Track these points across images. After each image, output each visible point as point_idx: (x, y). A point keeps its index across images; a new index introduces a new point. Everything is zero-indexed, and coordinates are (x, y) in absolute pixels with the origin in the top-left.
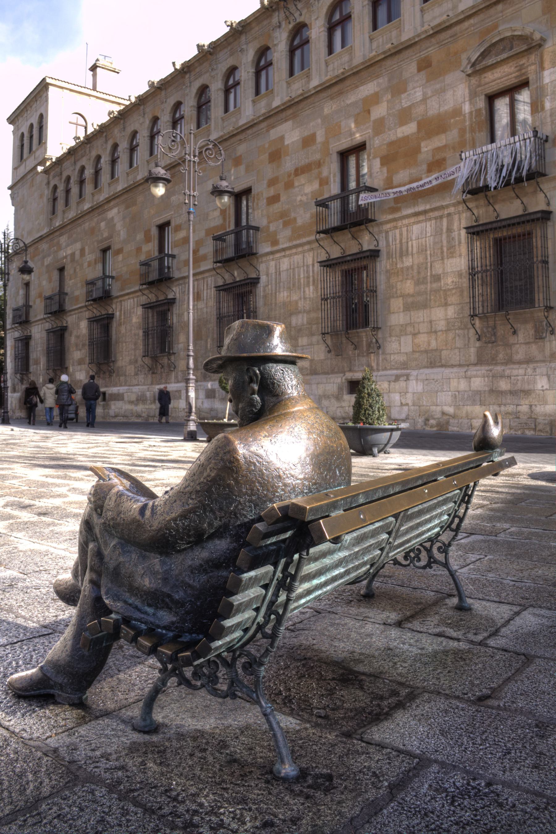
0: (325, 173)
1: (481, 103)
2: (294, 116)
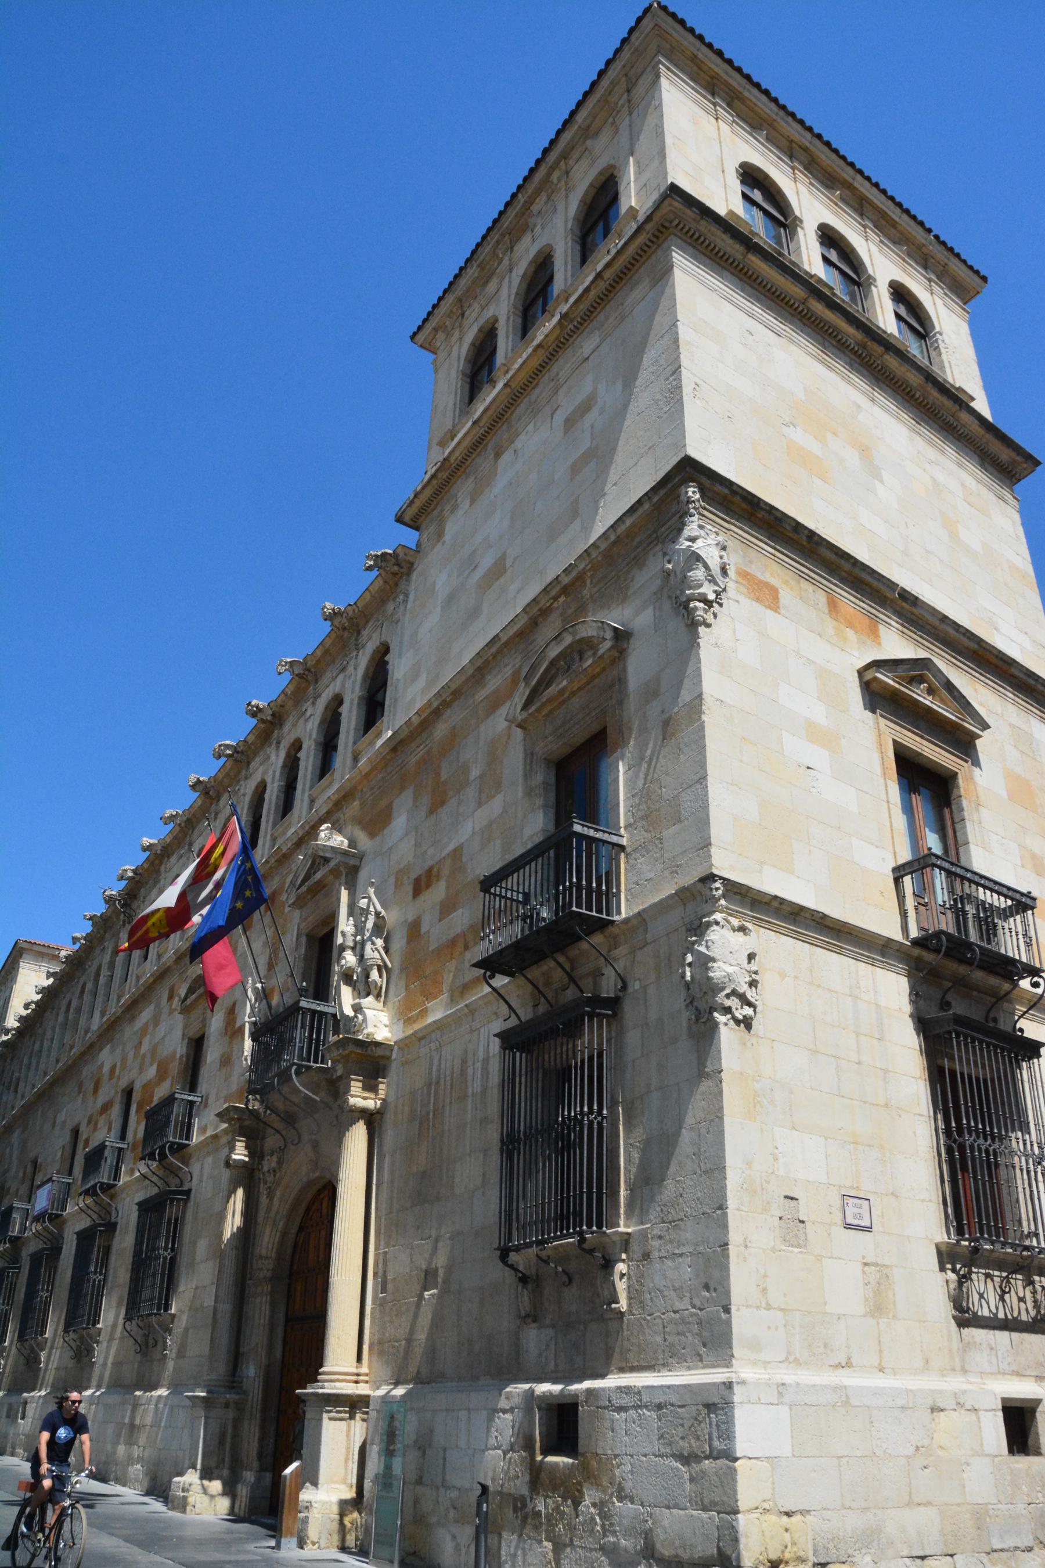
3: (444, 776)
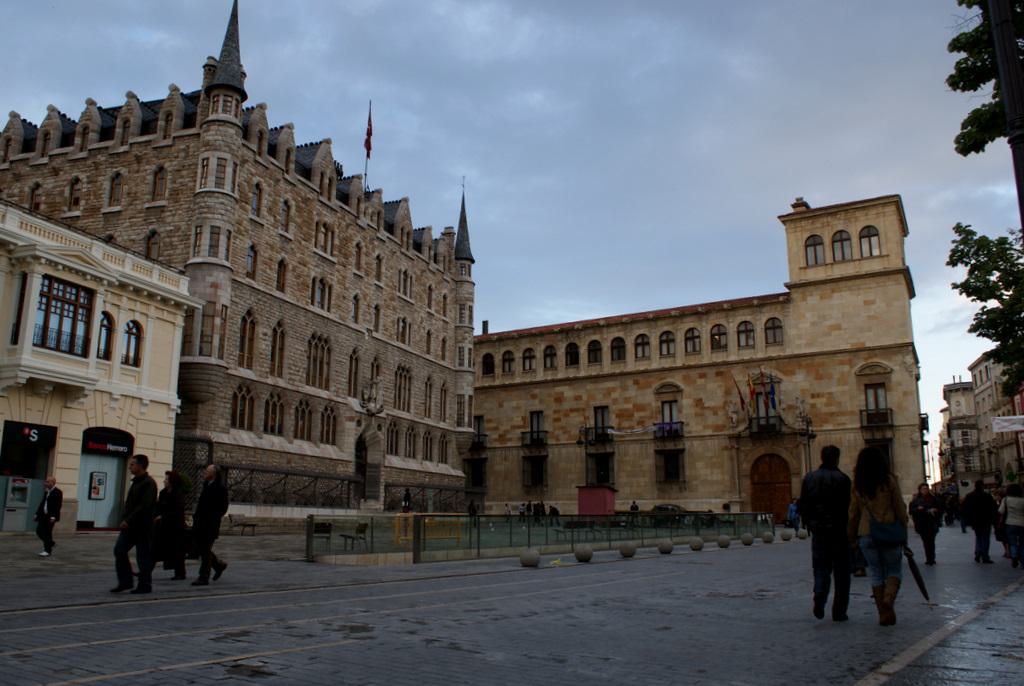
0: (587, 414)
1: (660, 404)
2: (569, 385)
3: (821, 372)
